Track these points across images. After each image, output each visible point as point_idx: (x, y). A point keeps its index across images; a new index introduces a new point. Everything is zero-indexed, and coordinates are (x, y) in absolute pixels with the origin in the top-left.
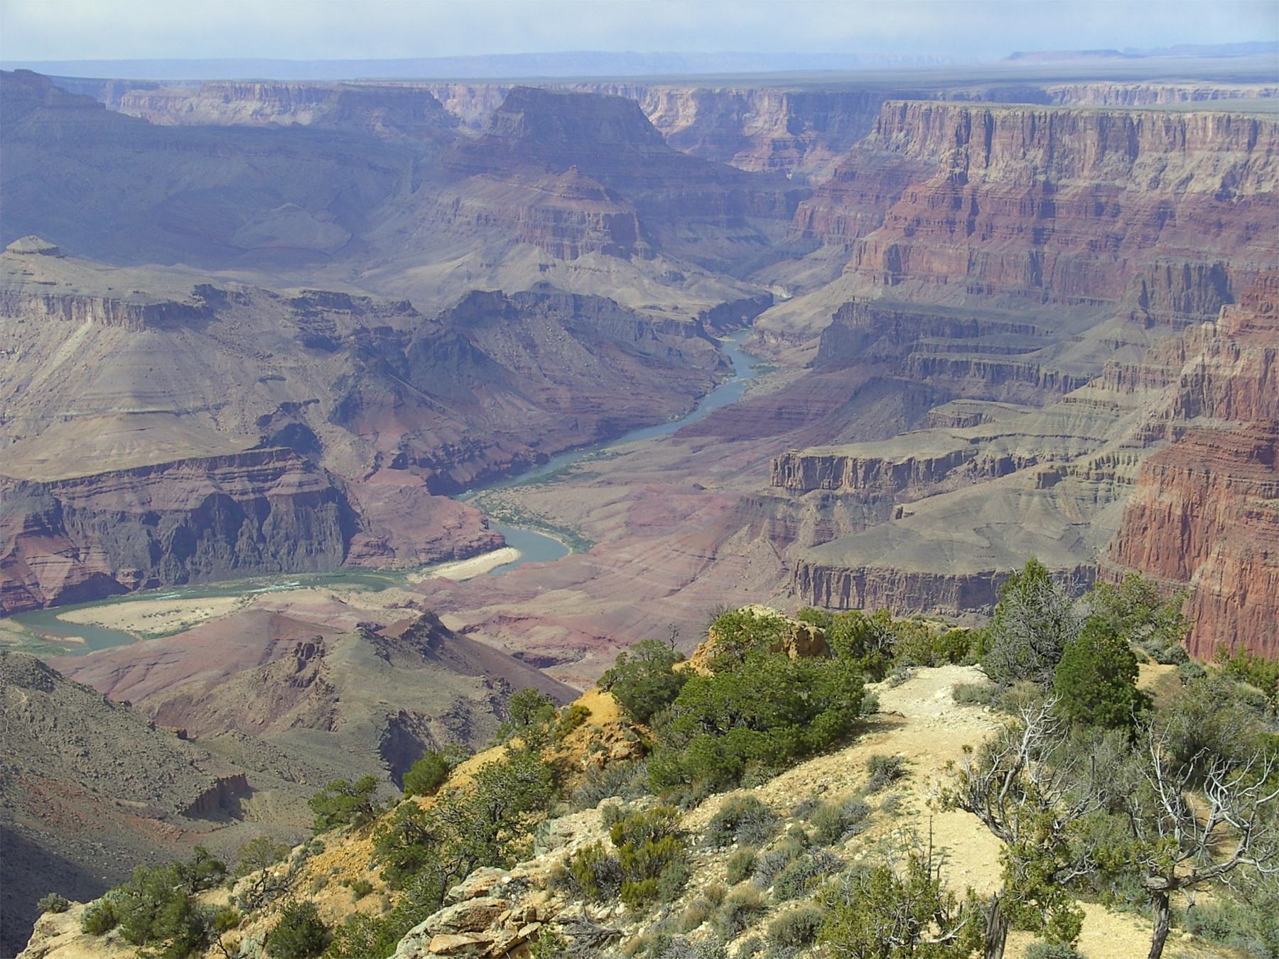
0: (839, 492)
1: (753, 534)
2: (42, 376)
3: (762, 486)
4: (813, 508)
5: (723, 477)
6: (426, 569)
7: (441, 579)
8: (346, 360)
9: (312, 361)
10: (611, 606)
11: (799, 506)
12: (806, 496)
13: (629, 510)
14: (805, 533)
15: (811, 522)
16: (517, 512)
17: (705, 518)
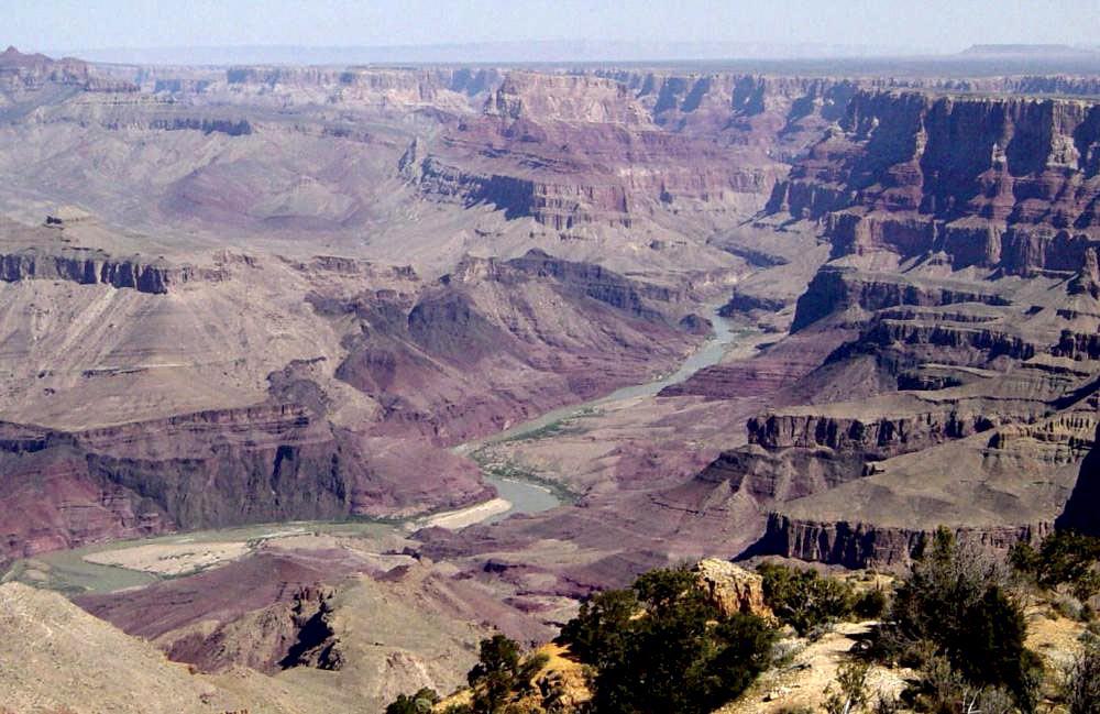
0: (813, 451)
1: (735, 488)
2: (75, 331)
3: (739, 441)
4: (789, 464)
5: (706, 434)
6: (421, 519)
7: (436, 529)
8: (353, 321)
9: (322, 323)
10: (594, 556)
11: (774, 463)
12: (782, 453)
13: (618, 464)
14: (783, 490)
15: (787, 478)
16: (510, 464)
17: (688, 473)
